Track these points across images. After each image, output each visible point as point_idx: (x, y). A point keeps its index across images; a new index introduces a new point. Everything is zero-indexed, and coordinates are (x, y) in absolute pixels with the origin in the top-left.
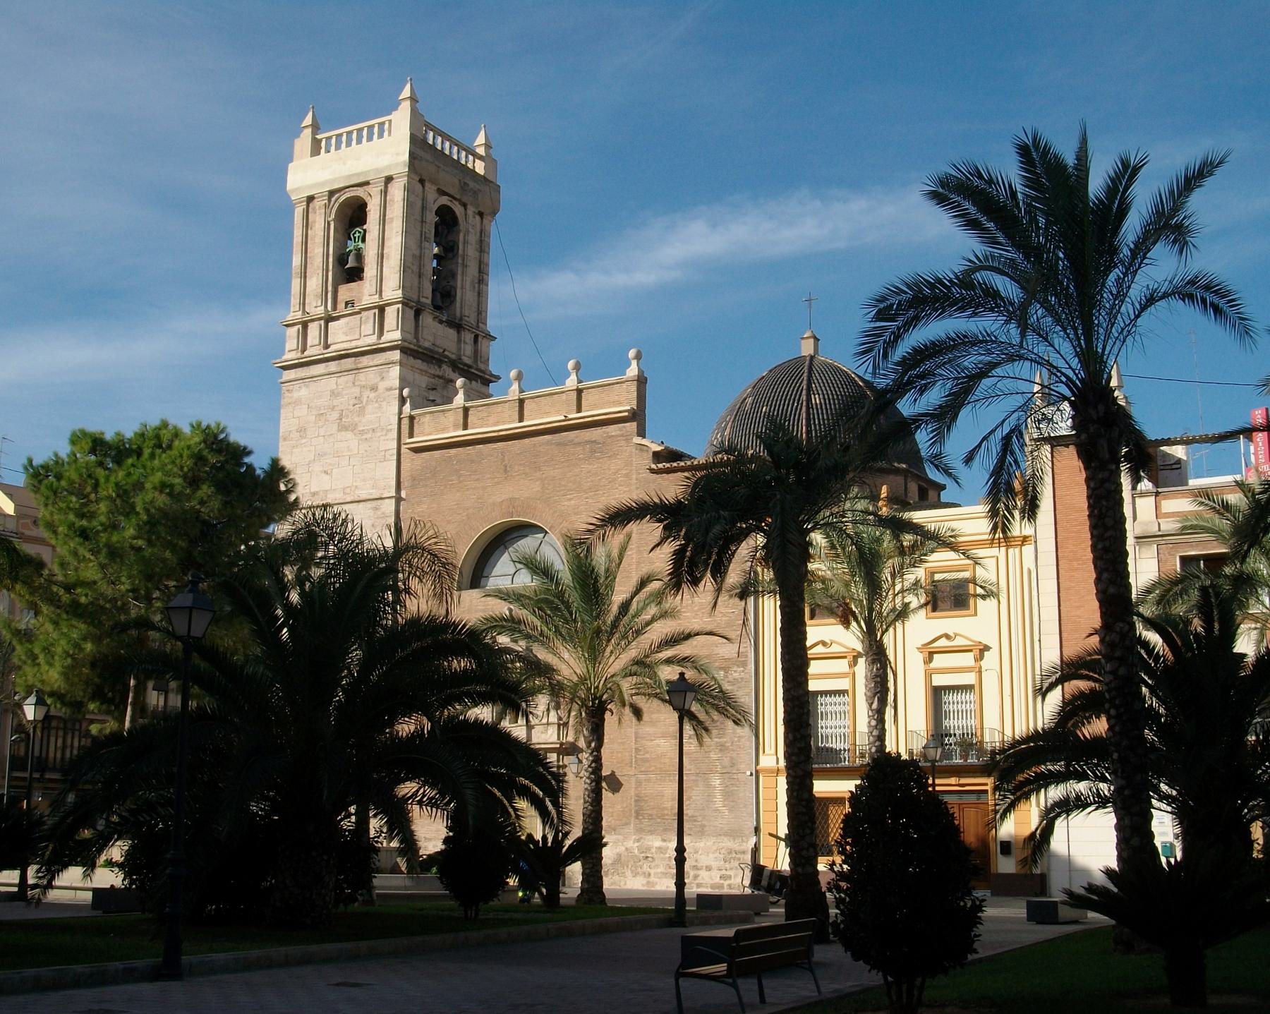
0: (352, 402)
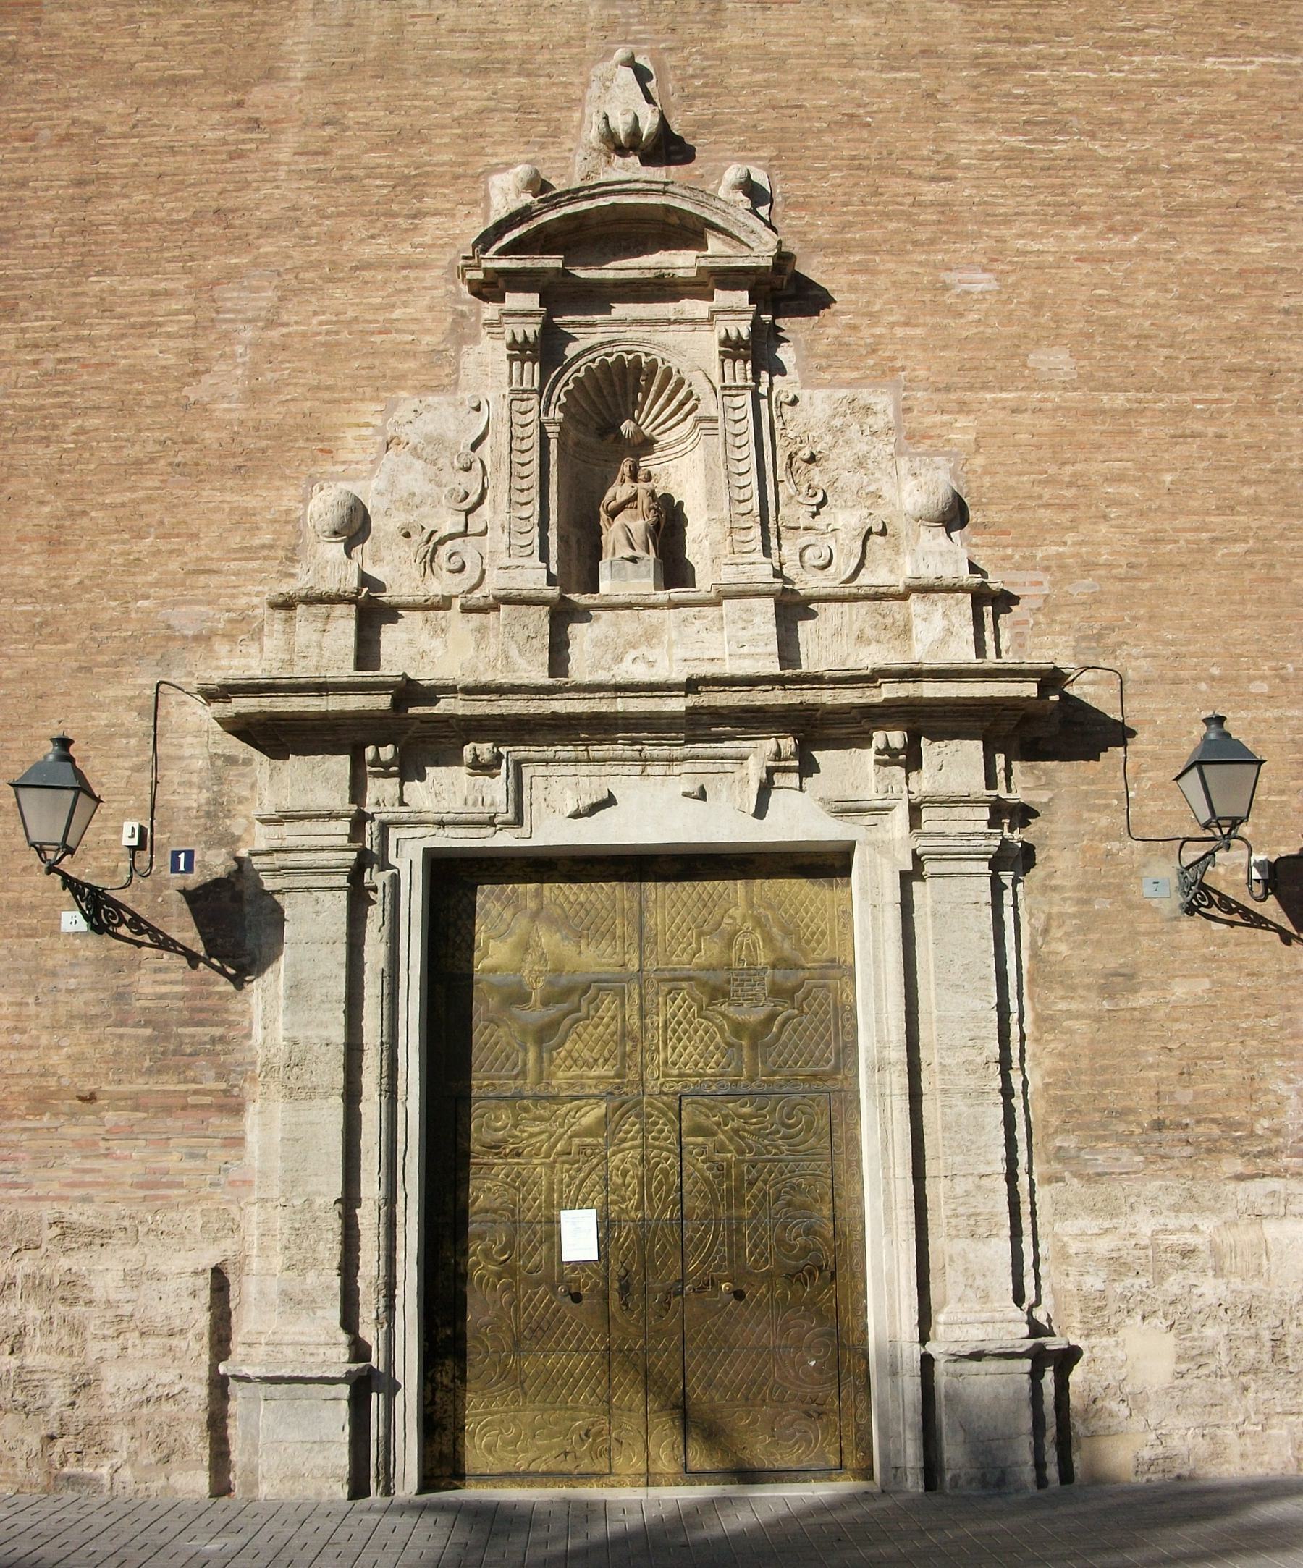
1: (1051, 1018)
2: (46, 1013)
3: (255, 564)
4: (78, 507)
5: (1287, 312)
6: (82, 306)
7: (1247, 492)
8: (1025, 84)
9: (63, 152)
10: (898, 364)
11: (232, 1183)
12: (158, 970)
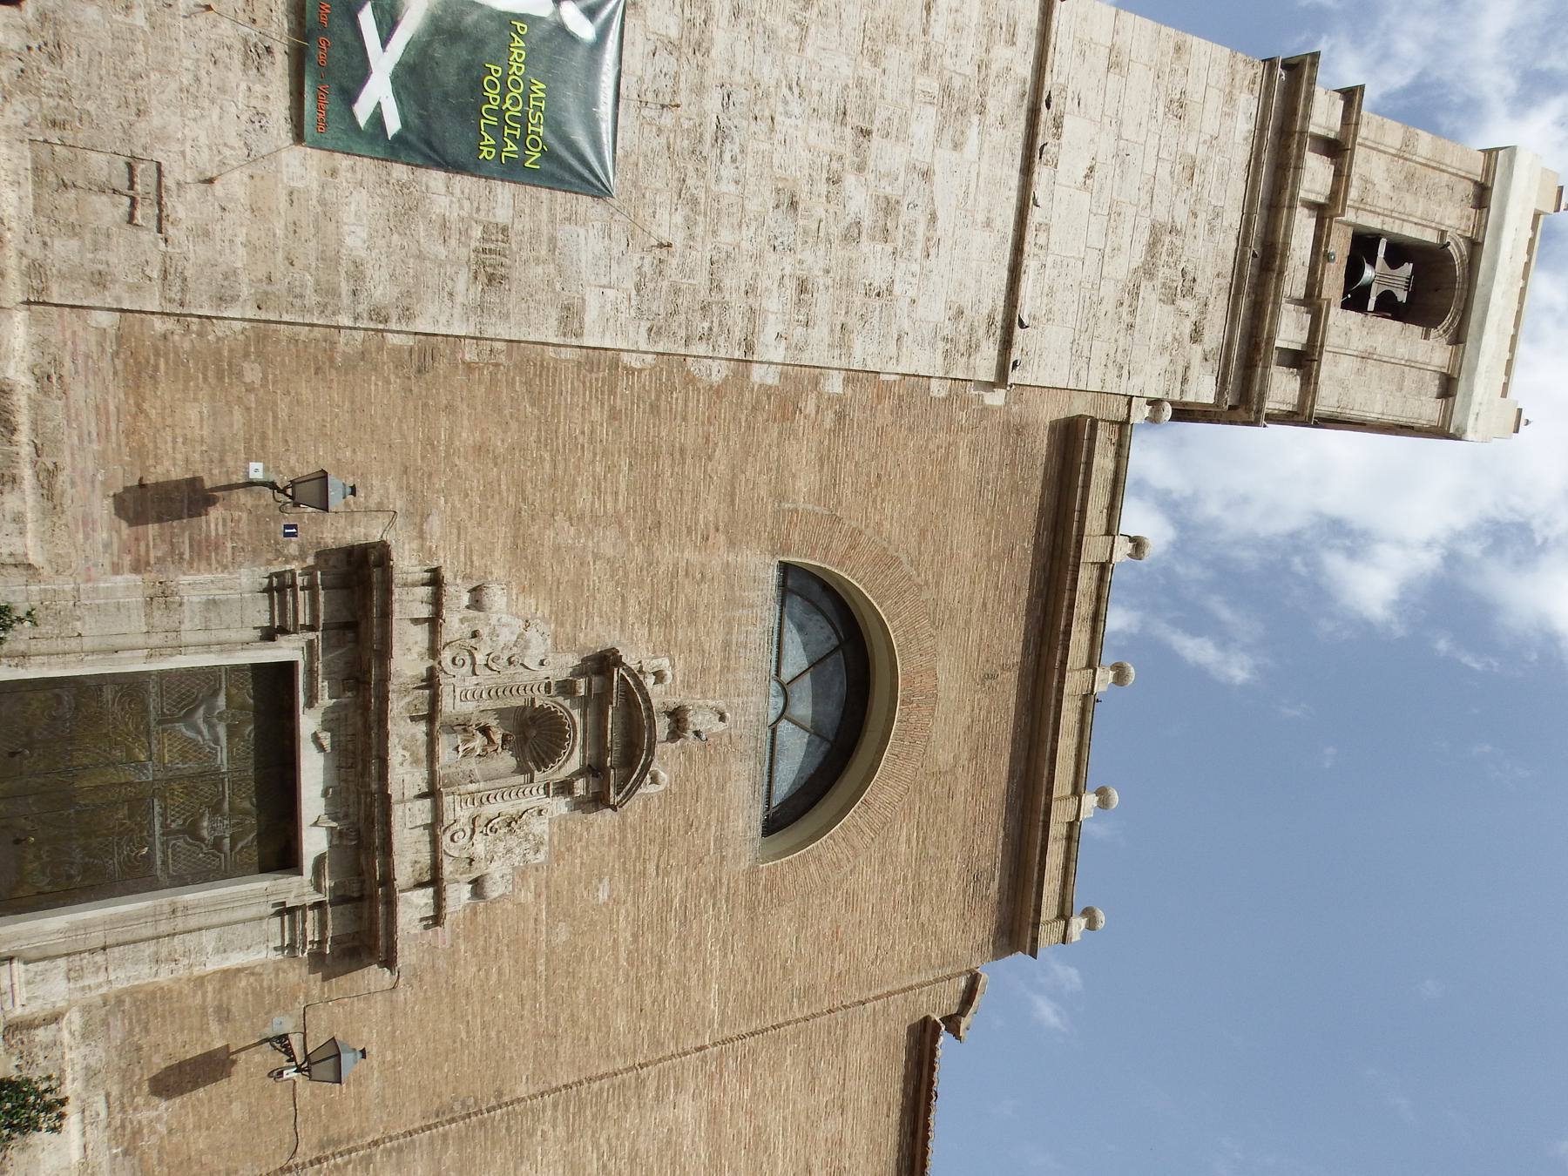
0: (1190, 268)
1: (202, 984)
2: (197, 456)
3: (462, 558)
4: (499, 461)
5: (587, 1039)
6: (613, 455)
7: (493, 1034)
8: (706, 902)
9: (700, 440)
10: (561, 863)
11: (89, 569)
12: (224, 520)
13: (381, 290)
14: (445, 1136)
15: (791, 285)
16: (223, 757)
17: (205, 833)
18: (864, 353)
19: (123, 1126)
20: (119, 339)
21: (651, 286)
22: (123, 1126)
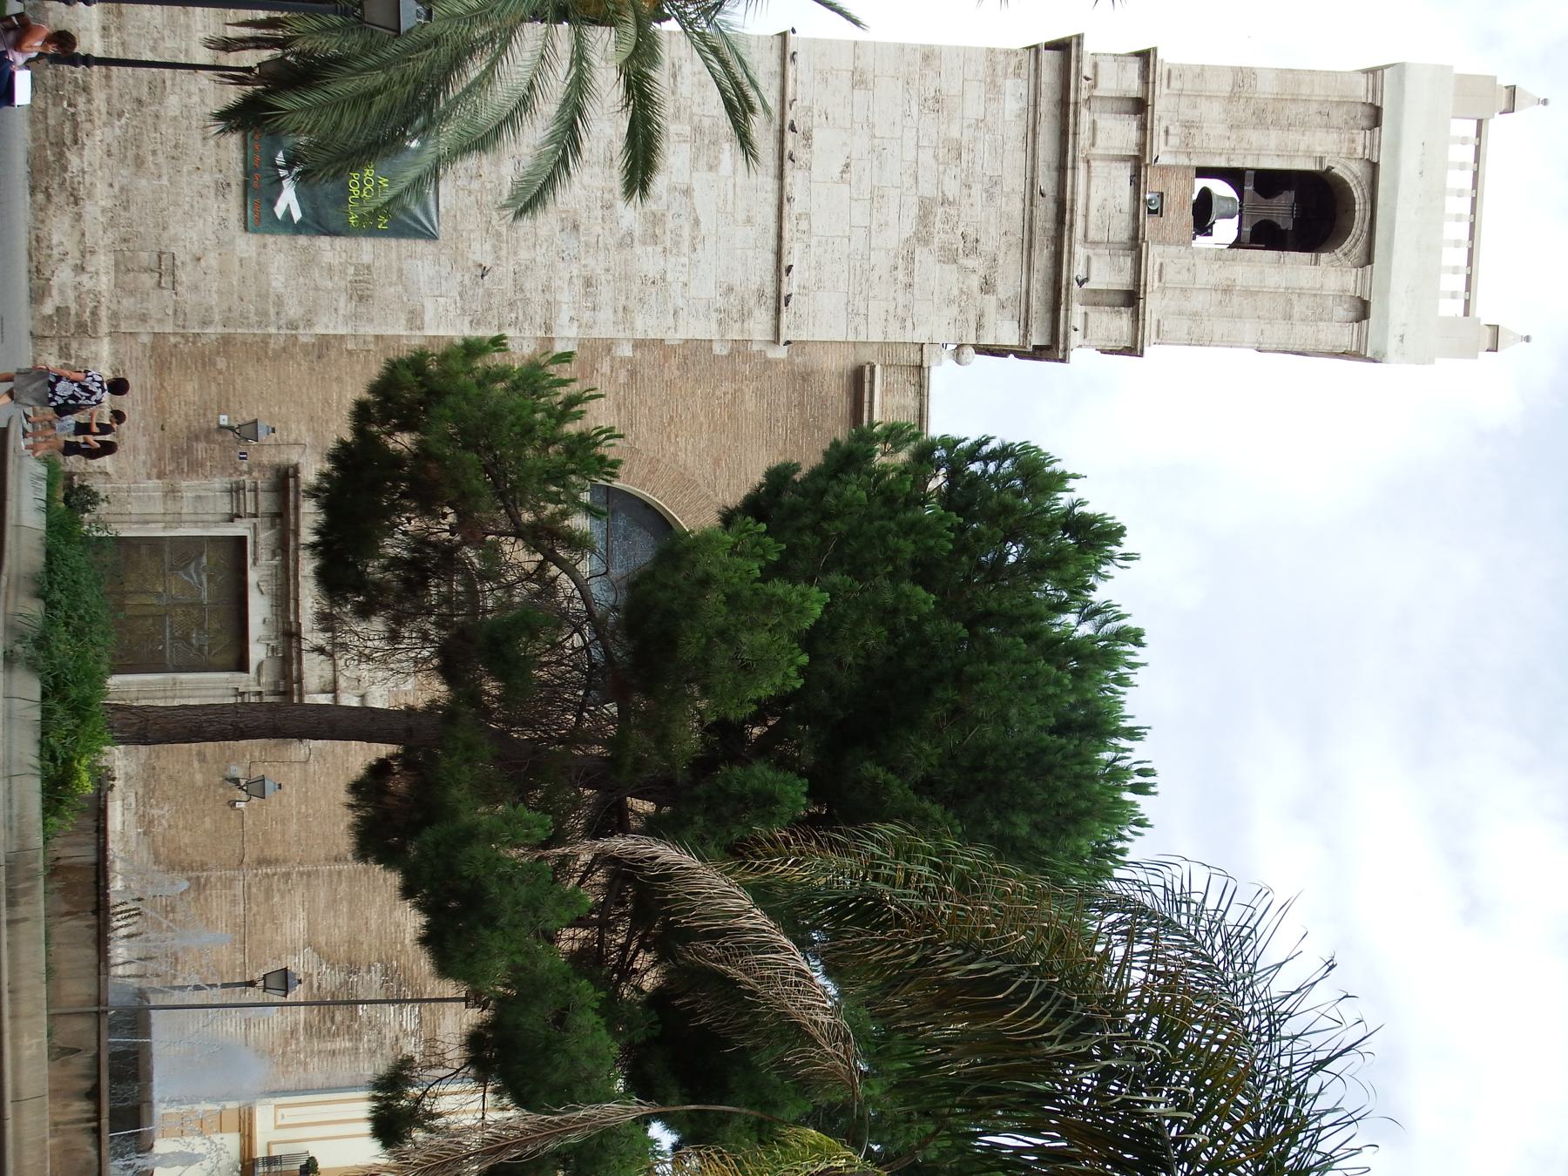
0: (970, 231)
2: (191, 413)
13: (293, 310)
14: (340, 873)
15: (578, 283)
16: (205, 594)
17: (194, 641)
18: (647, 325)
19: (144, 816)
20: (153, 348)
21: (470, 293)
22: (144, 816)
